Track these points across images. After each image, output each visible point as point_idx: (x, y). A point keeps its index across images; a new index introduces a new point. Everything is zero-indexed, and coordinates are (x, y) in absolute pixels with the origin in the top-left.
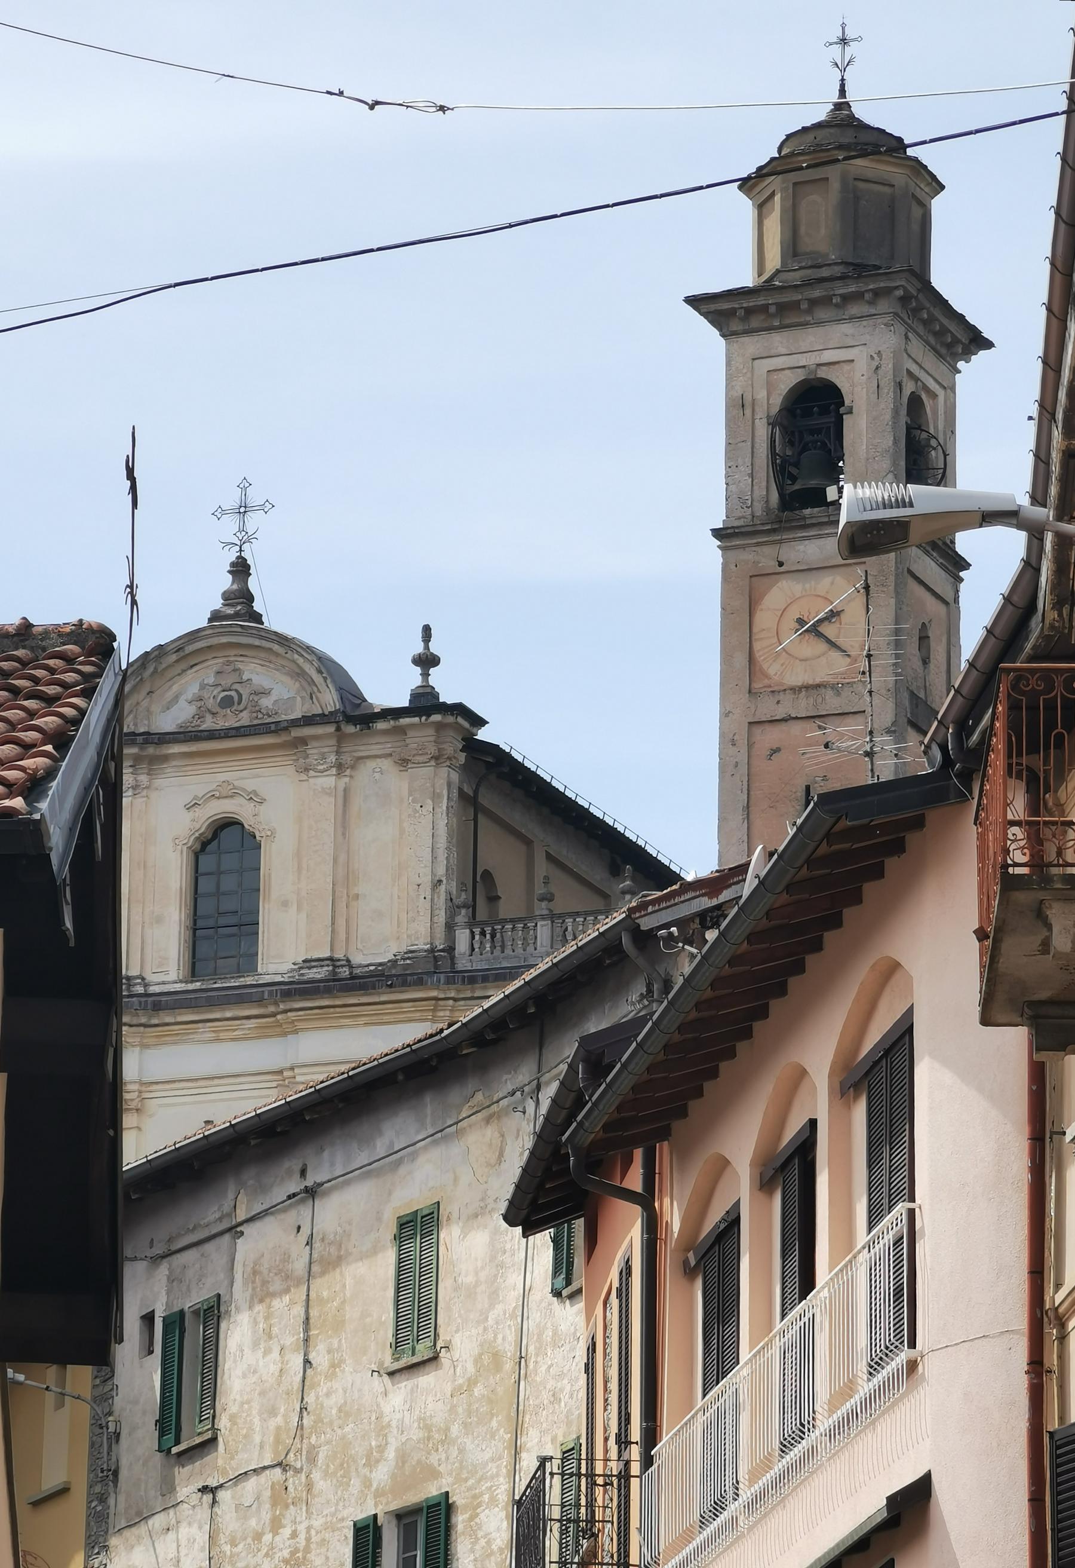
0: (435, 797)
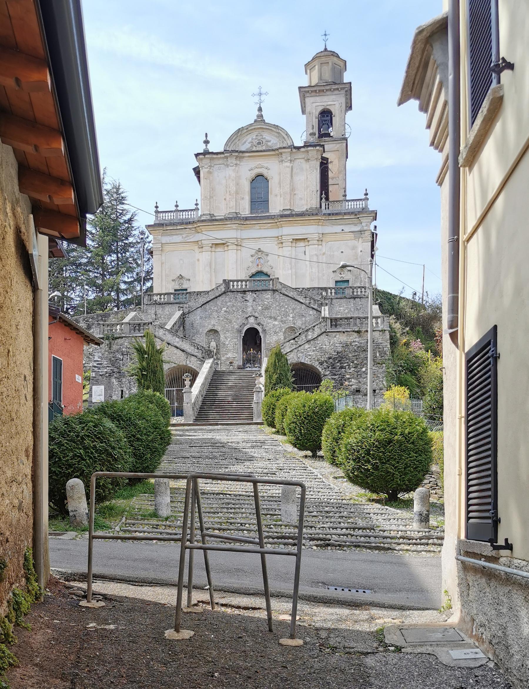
0: (317, 169)
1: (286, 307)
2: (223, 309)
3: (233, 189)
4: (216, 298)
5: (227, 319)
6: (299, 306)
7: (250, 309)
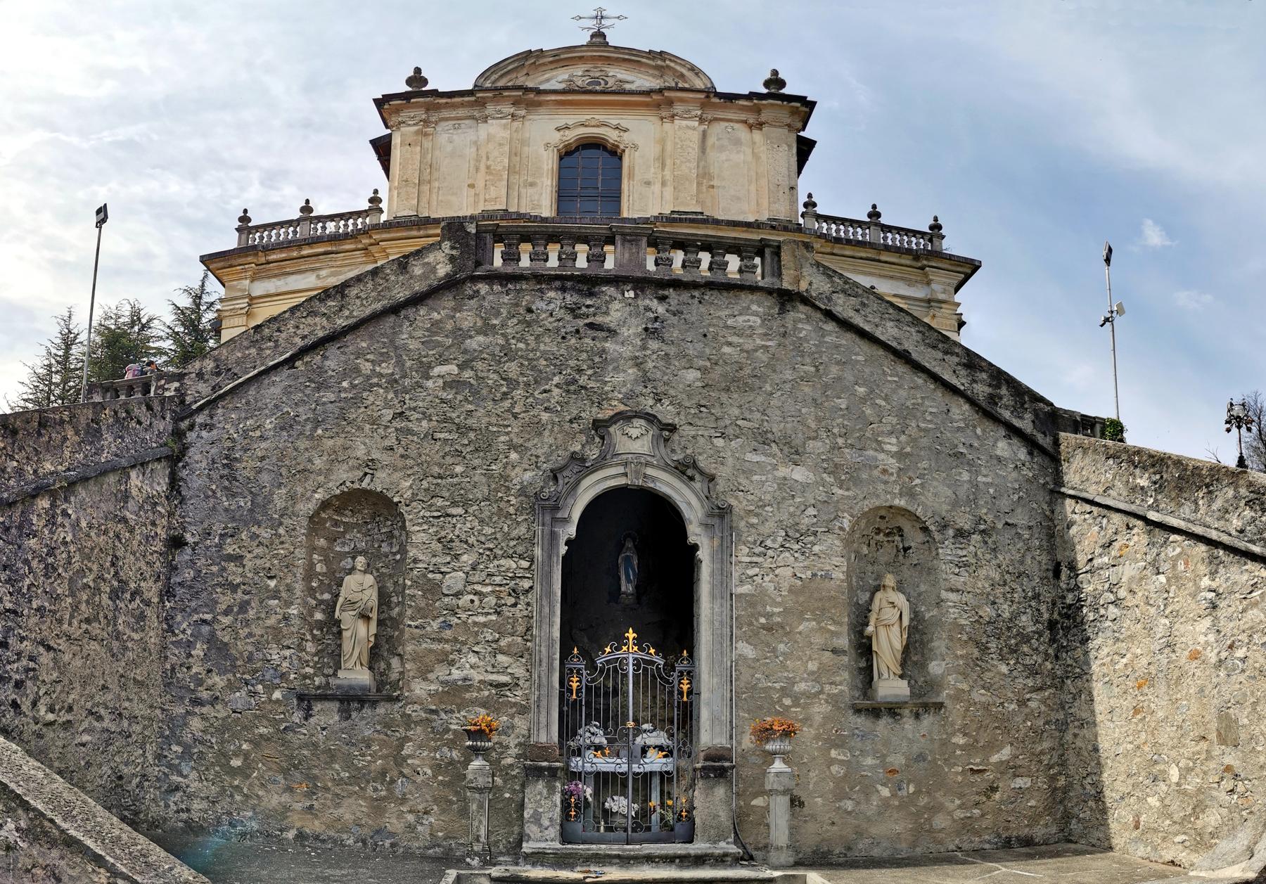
1: (861, 390)
2: (438, 370)
3: (501, 161)
4: (395, 309)
5: (462, 430)
6: (935, 401)
7: (622, 379)
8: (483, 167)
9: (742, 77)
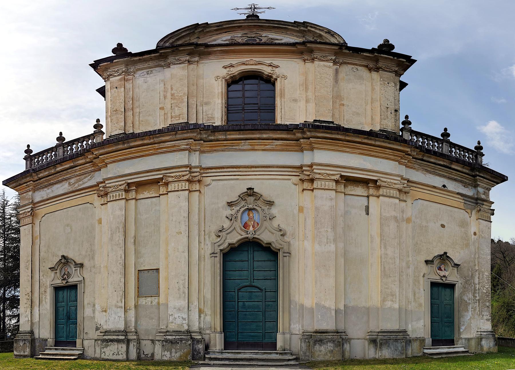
8: (169, 96)
9: (365, 37)
